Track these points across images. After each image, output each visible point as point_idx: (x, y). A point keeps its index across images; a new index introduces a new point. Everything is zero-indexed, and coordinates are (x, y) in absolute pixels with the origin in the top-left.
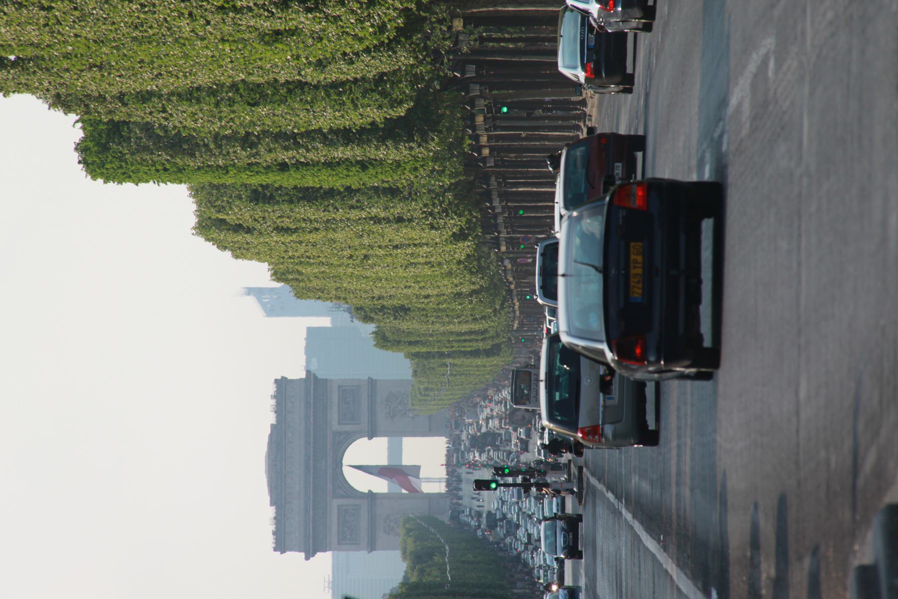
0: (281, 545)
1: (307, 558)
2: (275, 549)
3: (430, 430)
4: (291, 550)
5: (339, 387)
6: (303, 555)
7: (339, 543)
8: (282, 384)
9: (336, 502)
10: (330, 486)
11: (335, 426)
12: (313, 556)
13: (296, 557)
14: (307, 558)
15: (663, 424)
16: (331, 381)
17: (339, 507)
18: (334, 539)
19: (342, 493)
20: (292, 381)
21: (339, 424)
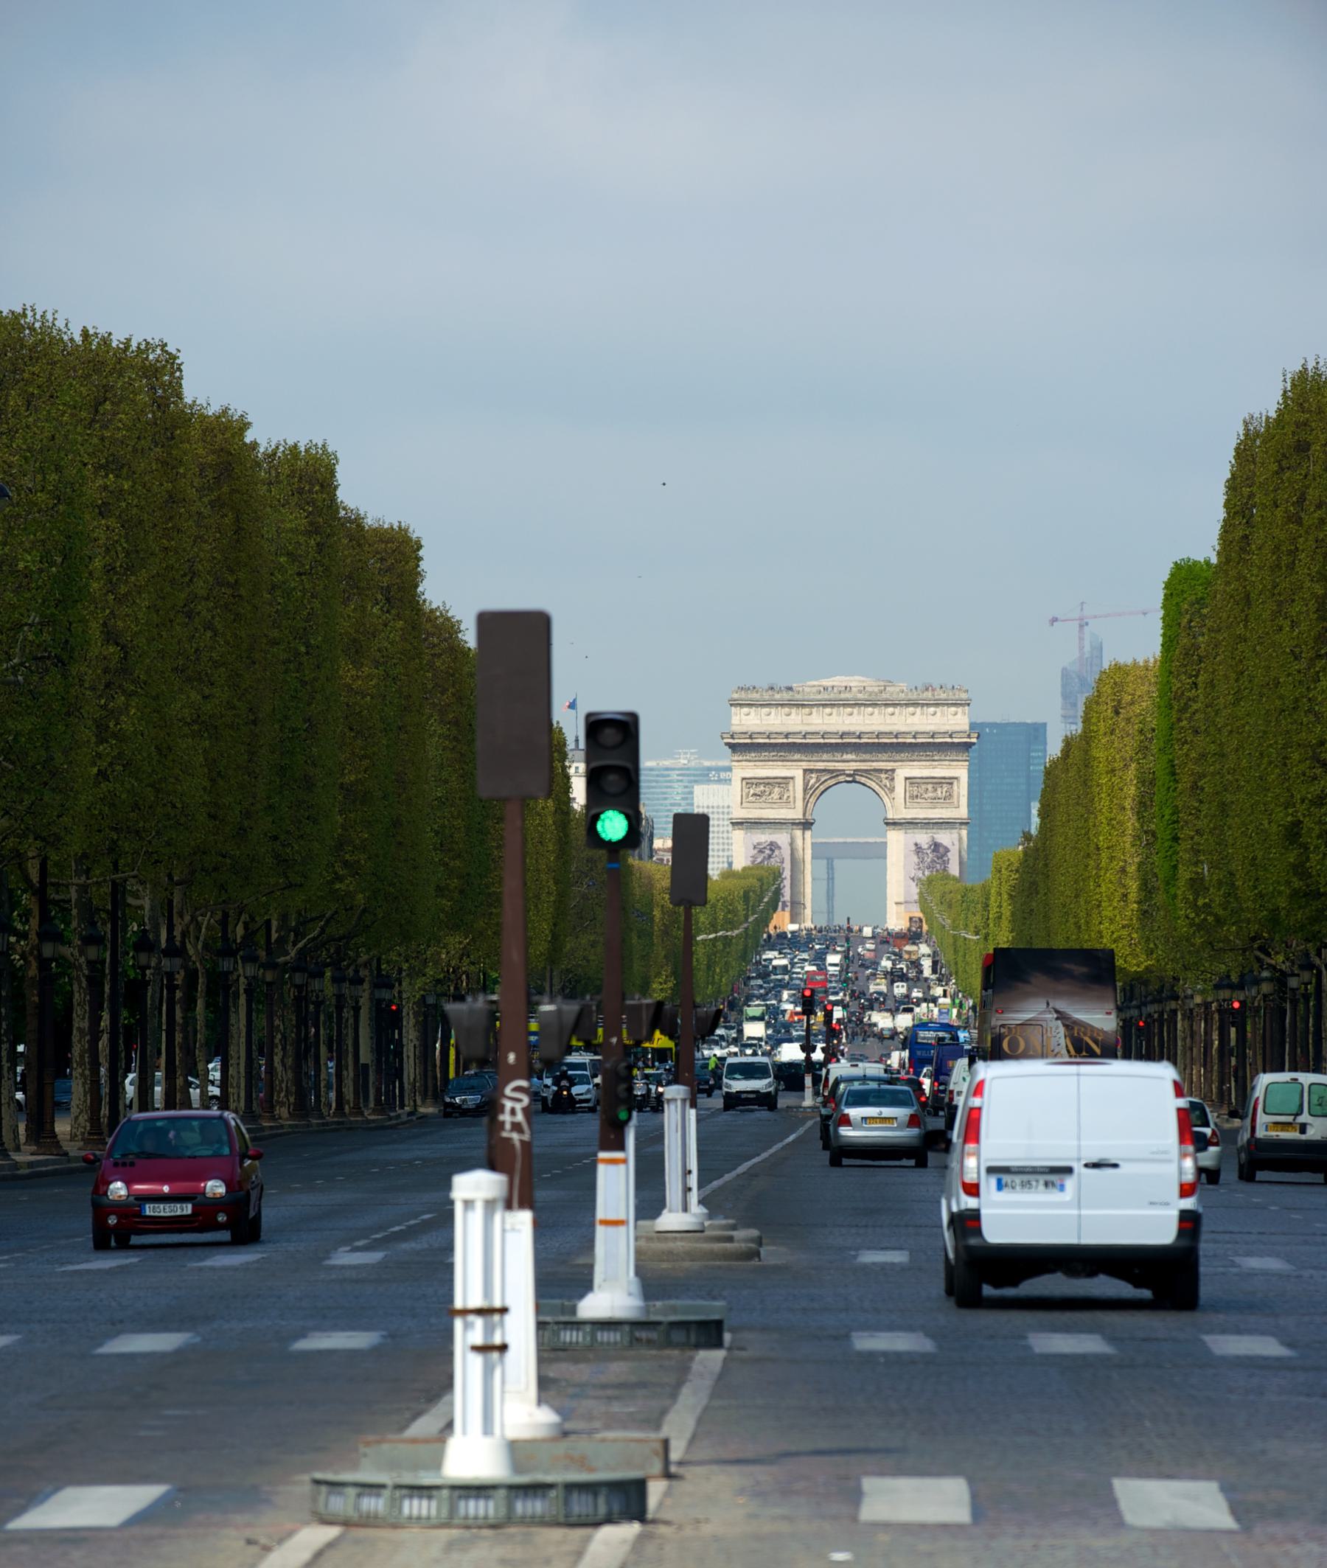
9: (798, 774)
10: (821, 765)
19: (812, 782)
21: (906, 779)
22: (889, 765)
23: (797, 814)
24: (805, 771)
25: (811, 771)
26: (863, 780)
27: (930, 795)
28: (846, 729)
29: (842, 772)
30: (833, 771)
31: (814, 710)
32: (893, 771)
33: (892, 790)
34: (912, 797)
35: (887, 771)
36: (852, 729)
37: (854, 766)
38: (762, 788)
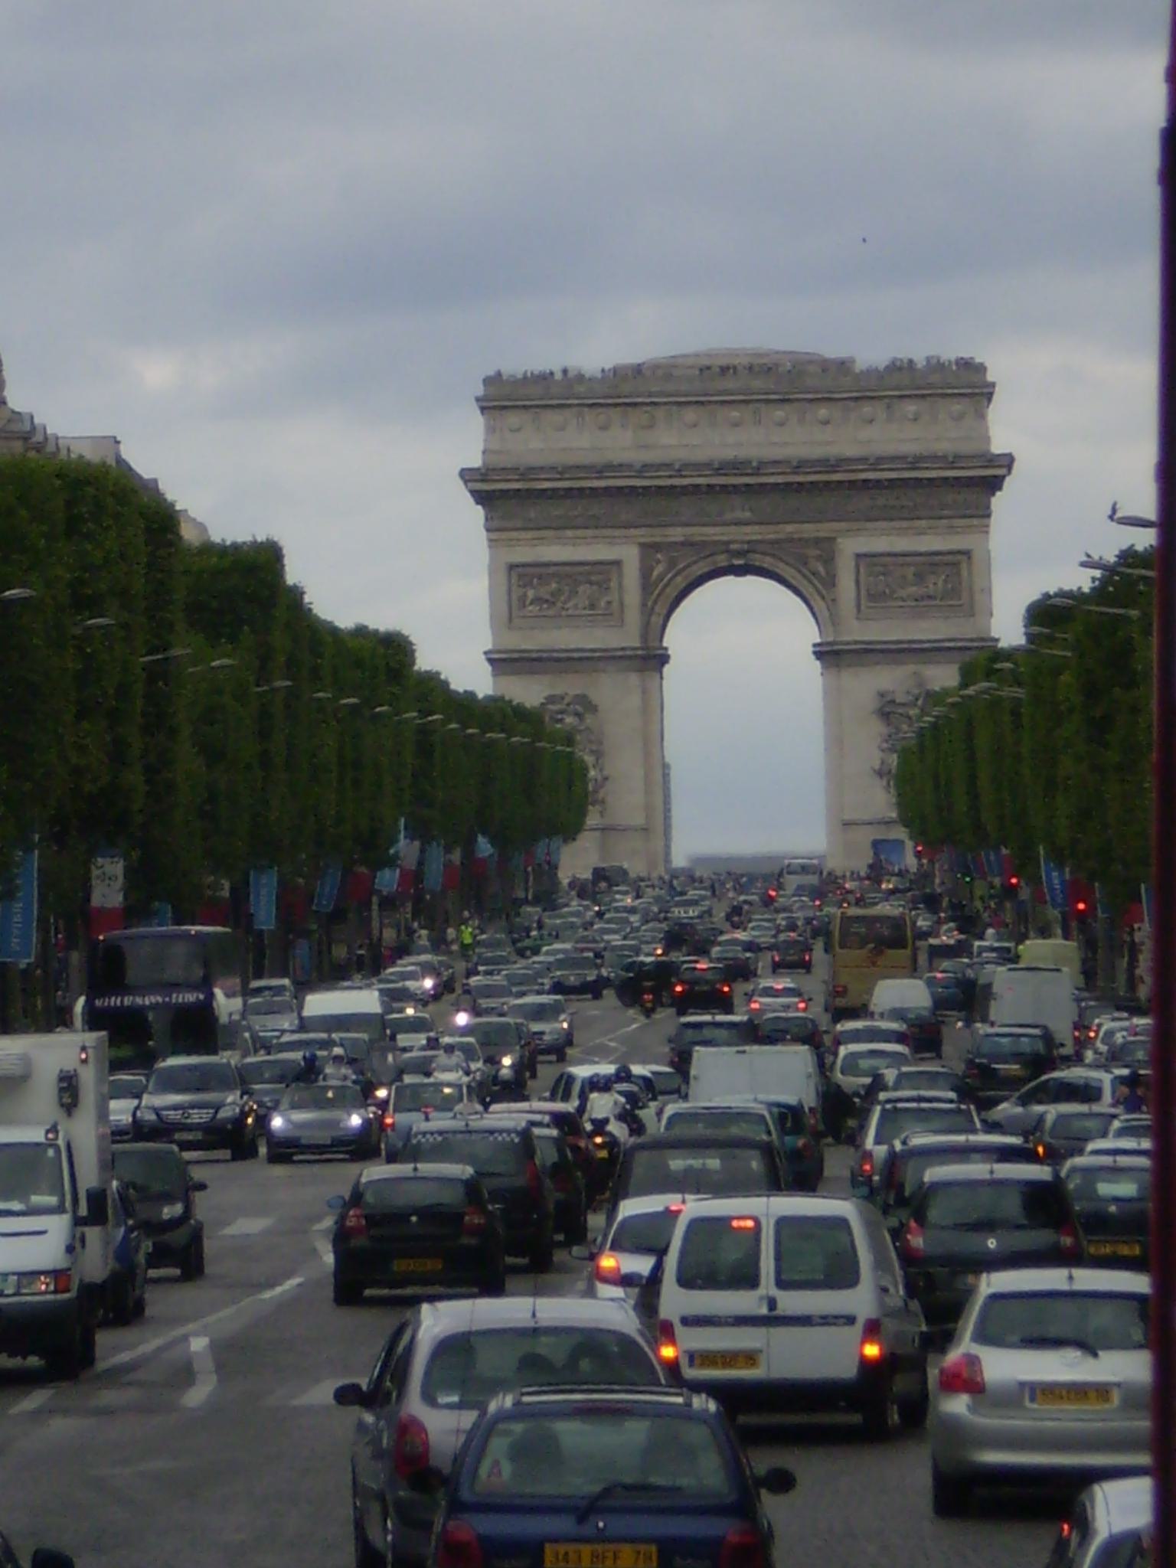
0: (506, 398)
1: (467, 475)
2: (488, 381)
3: (847, 824)
4: (490, 430)
5: (967, 553)
6: (476, 461)
7: (512, 567)
8: (967, 386)
9: (629, 555)
10: (677, 534)
11: (851, 545)
12: (473, 493)
13: (467, 441)
14: (467, 475)
15: (745, 1213)
16: (985, 530)
17: (617, 563)
18: (524, 554)
20: (982, 416)
21: (859, 556)
22: (823, 529)
23: (627, 637)
24: (649, 549)
25: (655, 547)
26: (767, 562)
27: (912, 590)
28: (729, 454)
29: (725, 547)
30: (704, 544)
31: (660, 413)
32: (832, 540)
33: (830, 581)
34: (871, 597)
35: (817, 541)
36: (743, 453)
37: (753, 533)
38: (554, 585)
